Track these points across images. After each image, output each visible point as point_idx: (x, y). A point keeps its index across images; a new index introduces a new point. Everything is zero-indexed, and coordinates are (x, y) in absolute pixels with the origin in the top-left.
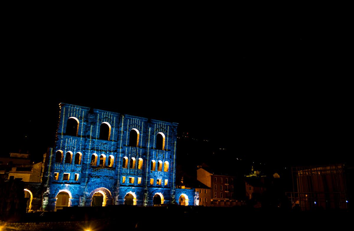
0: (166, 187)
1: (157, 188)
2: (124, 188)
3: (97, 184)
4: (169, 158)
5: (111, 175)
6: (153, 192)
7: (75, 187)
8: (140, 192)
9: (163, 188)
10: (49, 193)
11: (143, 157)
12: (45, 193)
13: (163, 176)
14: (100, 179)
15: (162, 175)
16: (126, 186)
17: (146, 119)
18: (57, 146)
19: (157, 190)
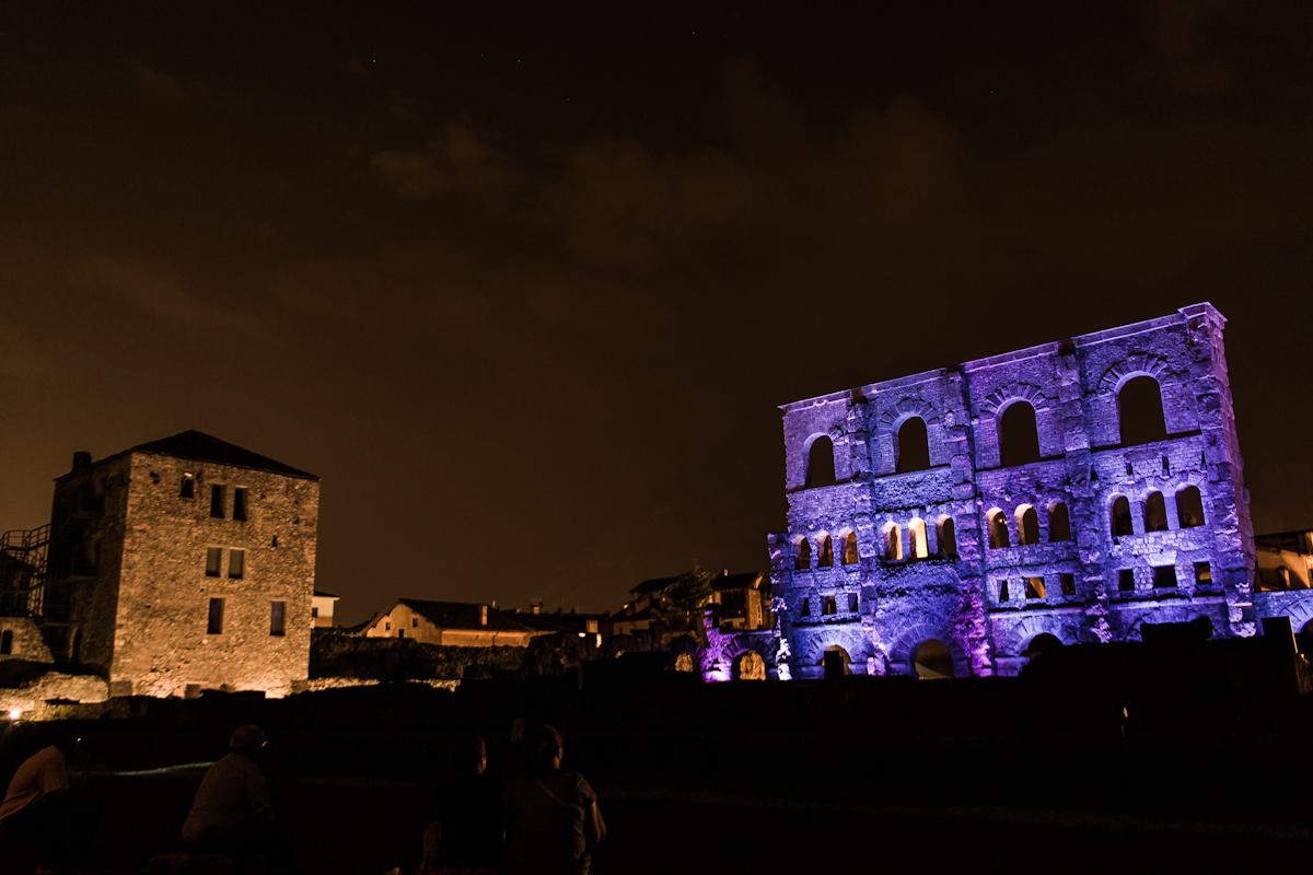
1: (1155, 604)
2: (1008, 620)
3: (902, 614)
4: (1198, 467)
5: (945, 580)
7: (853, 631)
9: (1183, 597)
10: (788, 653)
11: (1065, 492)
13: (1179, 550)
14: (904, 599)
15: (1170, 548)
16: (1016, 610)
17: (1052, 348)
18: (789, 525)
19: (1156, 609)
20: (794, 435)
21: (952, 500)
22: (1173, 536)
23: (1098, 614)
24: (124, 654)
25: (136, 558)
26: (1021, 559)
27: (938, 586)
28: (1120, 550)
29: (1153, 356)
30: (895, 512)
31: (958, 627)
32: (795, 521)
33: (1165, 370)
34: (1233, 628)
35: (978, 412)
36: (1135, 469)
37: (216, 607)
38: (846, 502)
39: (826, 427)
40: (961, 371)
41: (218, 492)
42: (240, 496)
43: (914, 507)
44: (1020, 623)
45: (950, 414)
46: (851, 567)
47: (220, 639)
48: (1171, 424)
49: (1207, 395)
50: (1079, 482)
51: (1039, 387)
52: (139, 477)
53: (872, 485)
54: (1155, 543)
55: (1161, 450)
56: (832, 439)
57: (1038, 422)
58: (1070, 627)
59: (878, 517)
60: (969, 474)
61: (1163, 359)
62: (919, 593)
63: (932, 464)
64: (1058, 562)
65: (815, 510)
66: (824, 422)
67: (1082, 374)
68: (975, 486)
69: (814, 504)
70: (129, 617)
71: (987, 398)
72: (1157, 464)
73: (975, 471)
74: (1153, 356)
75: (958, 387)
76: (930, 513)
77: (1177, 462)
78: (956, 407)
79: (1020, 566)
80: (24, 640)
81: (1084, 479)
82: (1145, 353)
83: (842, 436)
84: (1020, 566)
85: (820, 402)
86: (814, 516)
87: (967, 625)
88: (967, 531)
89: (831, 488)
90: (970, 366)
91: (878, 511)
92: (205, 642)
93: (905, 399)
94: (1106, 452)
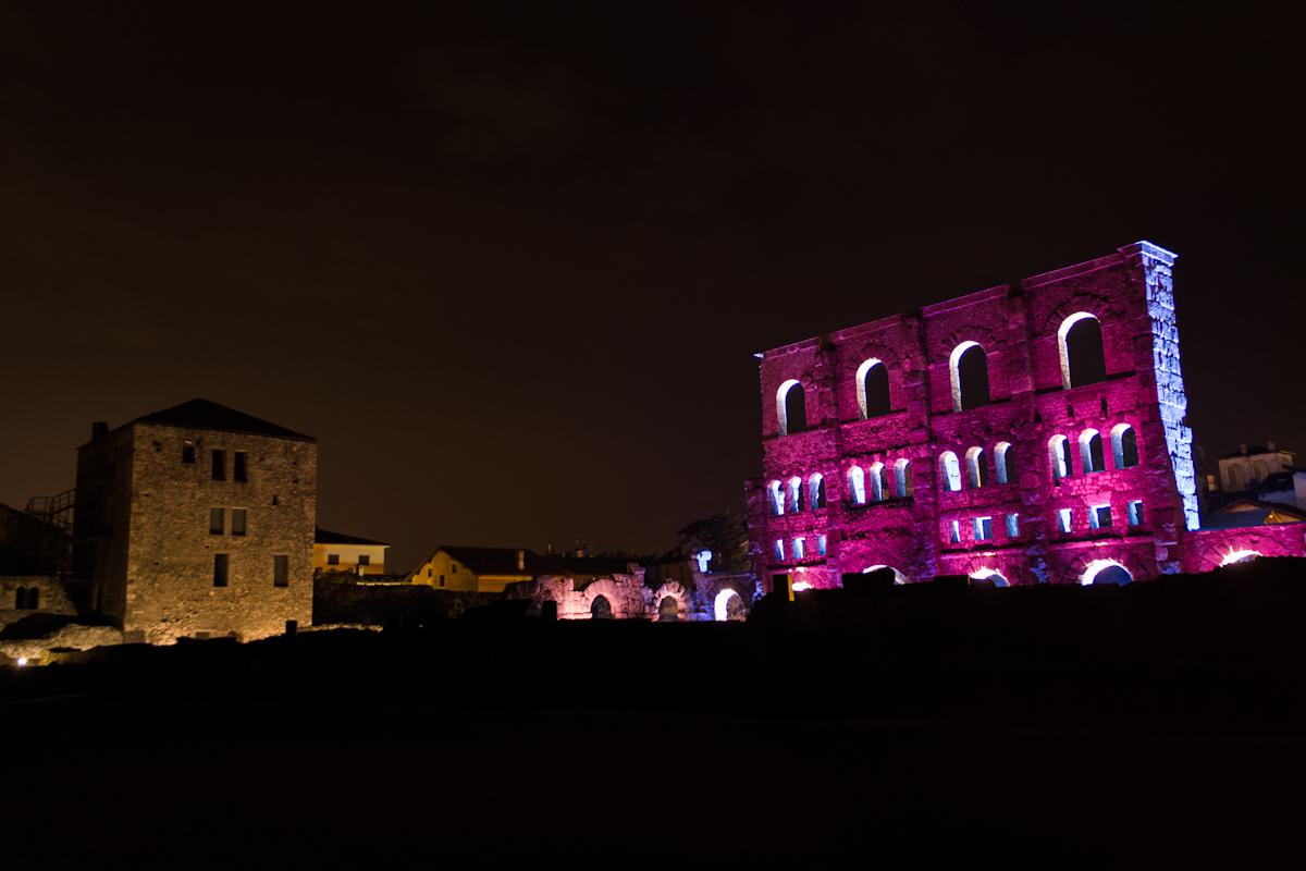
0: (1134, 532)
1: (1089, 544)
2: (958, 560)
6: (1076, 559)
8: (1021, 566)
12: (755, 595)
13: (1113, 490)
14: (863, 542)
15: (1105, 488)
16: (965, 551)
17: (1003, 290)
18: (764, 471)
20: (770, 383)
21: (909, 444)
22: (1108, 477)
23: (1037, 553)
24: (136, 606)
25: (144, 519)
26: (971, 502)
27: (896, 529)
28: (1060, 491)
29: (1095, 297)
30: (859, 457)
31: (911, 568)
32: (770, 467)
33: (1107, 310)
34: (1159, 567)
35: (935, 358)
36: (1076, 410)
37: (221, 564)
38: (815, 448)
39: (799, 373)
40: (918, 315)
41: (218, 457)
42: (240, 460)
43: (876, 452)
44: (969, 564)
45: (907, 360)
46: (820, 512)
47: (226, 590)
48: (1111, 365)
49: (1141, 336)
50: (1022, 425)
51: (990, 330)
52: (143, 447)
53: (839, 430)
54: (1093, 484)
55: (1100, 391)
56: (804, 386)
57: (989, 366)
58: (1015, 568)
59: (843, 462)
60: (925, 417)
61: (1105, 299)
62: (877, 534)
63: (892, 409)
64: (1004, 503)
65: (788, 456)
66: (797, 369)
67: (1028, 317)
68: (930, 430)
69: (787, 450)
70: (139, 574)
71: (943, 342)
72: (1095, 406)
73: (931, 415)
74: (1095, 297)
75: (914, 332)
76: (890, 457)
77: (1113, 404)
78: (913, 352)
79: (969, 508)
80: (49, 596)
81: (1027, 421)
82: (1089, 293)
83: (812, 382)
84: (969, 508)
85: (792, 349)
86: (786, 462)
87: (920, 566)
88: (920, 475)
89: (801, 434)
90: (928, 311)
91: (844, 457)
92: (212, 593)
93: (869, 345)
94: (1050, 394)
